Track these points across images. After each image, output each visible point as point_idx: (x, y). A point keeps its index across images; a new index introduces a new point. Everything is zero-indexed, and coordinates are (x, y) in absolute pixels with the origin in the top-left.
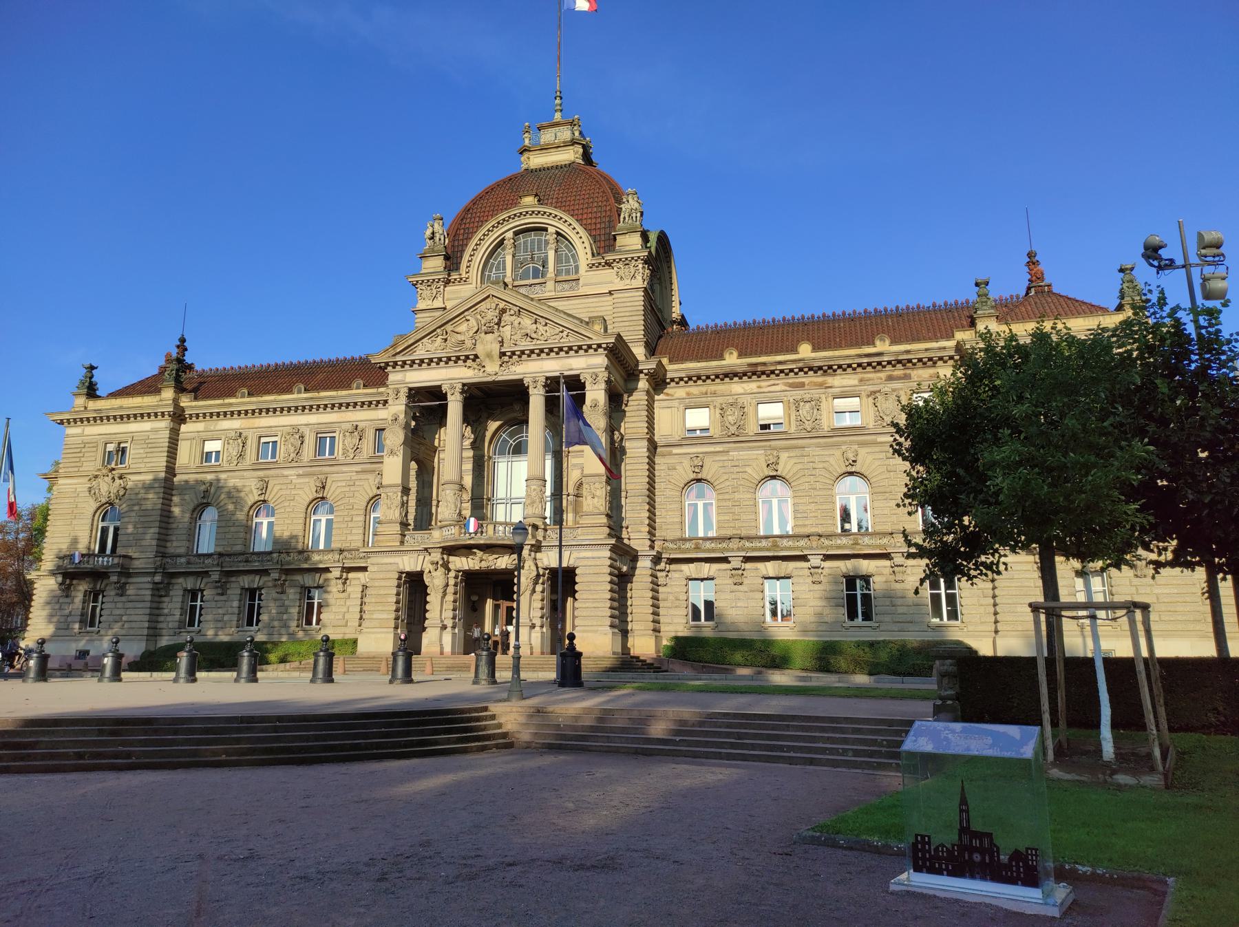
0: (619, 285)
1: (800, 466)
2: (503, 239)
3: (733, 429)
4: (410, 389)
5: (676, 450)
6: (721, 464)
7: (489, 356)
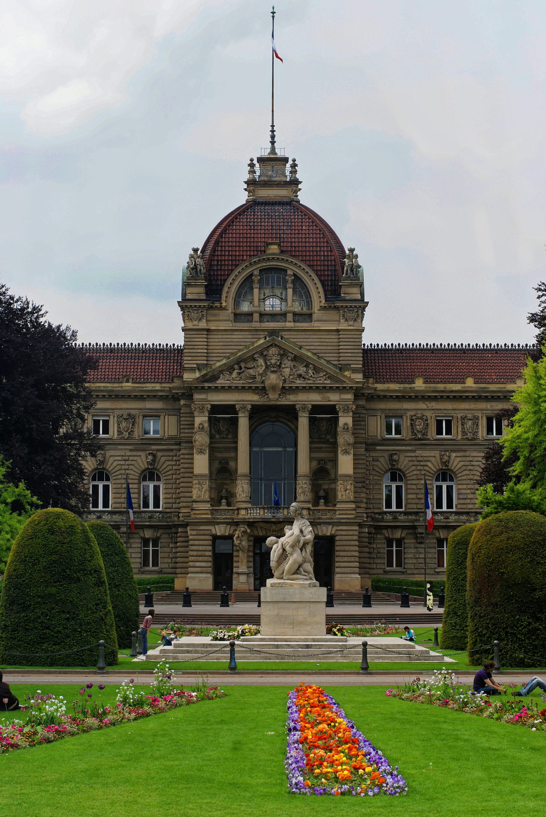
0: (343, 326)
1: (463, 463)
2: (252, 275)
3: (420, 436)
4: (213, 406)
5: (378, 448)
6: (410, 459)
7: (274, 388)
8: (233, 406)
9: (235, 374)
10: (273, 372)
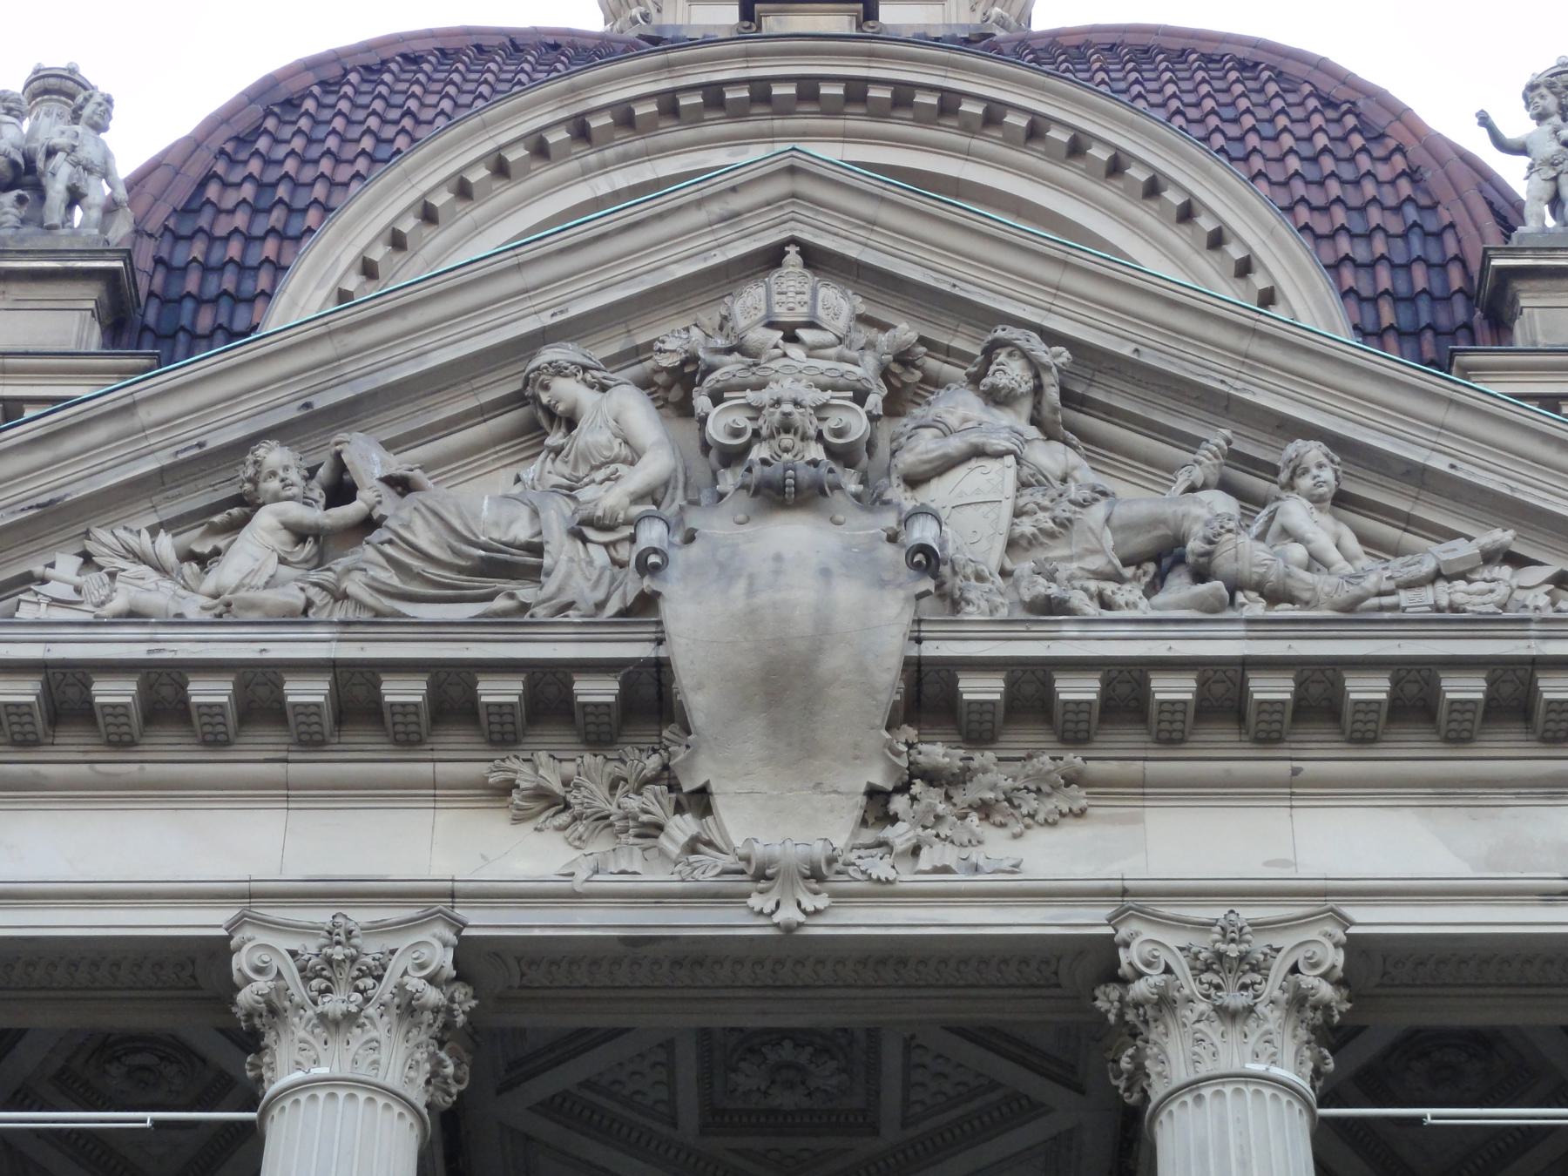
7: (784, 687)
8: (199, 968)
9: (253, 554)
10: (777, 495)
